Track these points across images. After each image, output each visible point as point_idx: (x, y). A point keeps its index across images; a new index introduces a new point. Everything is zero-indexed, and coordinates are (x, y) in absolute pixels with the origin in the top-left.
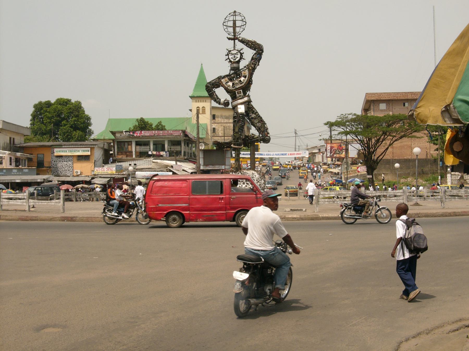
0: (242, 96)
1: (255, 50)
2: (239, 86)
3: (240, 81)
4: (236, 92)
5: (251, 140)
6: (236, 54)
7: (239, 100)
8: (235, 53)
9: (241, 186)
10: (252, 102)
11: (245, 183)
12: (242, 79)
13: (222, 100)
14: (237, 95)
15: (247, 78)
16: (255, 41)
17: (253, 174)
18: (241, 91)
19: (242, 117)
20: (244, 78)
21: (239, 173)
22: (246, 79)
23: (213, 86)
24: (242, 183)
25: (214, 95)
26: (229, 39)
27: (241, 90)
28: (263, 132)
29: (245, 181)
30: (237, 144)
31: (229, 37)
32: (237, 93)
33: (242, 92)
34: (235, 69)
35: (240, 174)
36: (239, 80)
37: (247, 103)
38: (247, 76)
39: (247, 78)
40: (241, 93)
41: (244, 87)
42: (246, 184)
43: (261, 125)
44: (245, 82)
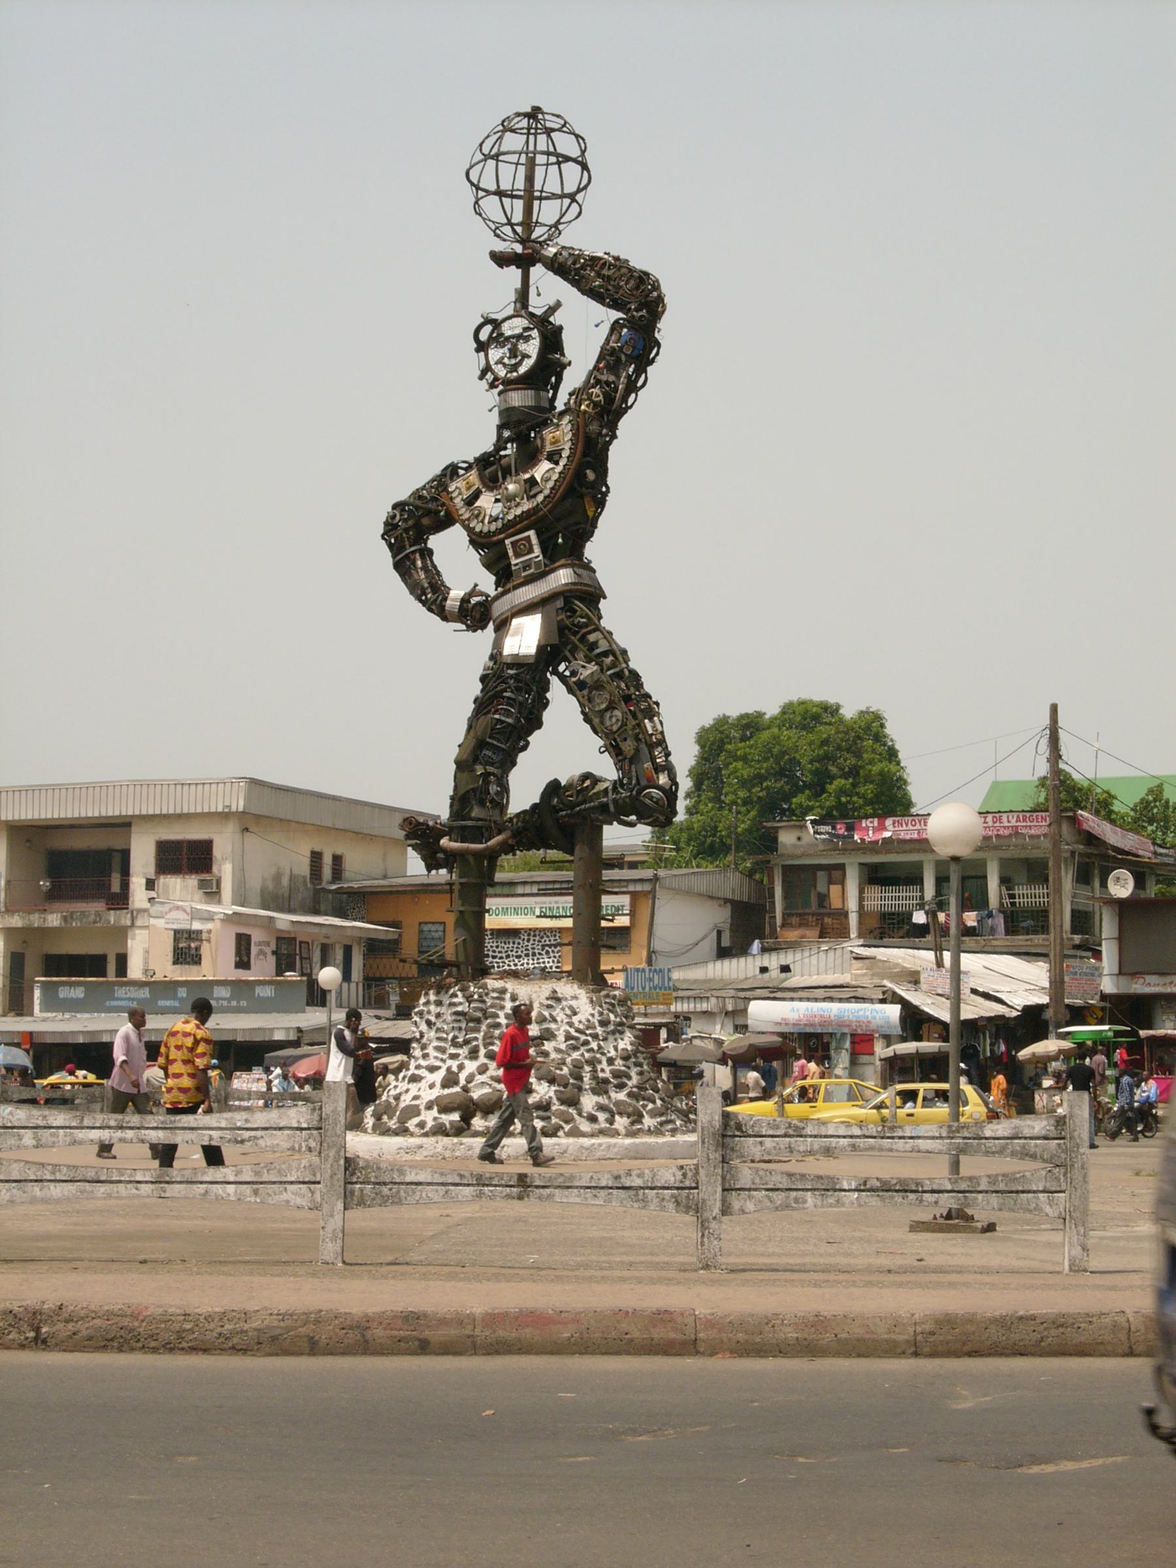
0: (538, 564)
1: (616, 305)
2: (518, 511)
3: (532, 482)
4: (507, 542)
5: (572, 806)
6: (519, 337)
7: (523, 589)
8: (518, 331)
9: (455, 1069)
10: (605, 597)
11: (482, 1051)
12: (541, 470)
13: (453, 594)
14: (514, 561)
15: (562, 462)
16: (617, 259)
17: (558, 1000)
18: (528, 538)
19: (516, 677)
20: (552, 466)
21: (454, 995)
22: (559, 468)
23: (410, 523)
24: (463, 1052)
25: (416, 568)
26: (501, 260)
27: (532, 533)
28: (631, 763)
29: (480, 1042)
30: (463, 828)
31: (500, 246)
32: (510, 552)
33: (534, 540)
34: (514, 418)
35: (460, 998)
36: (527, 476)
37: (560, 603)
38: (565, 454)
39: (562, 462)
40: (531, 551)
41: (545, 516)
42: (482, 1060)
43: (624, 724)
44: (550, 484)
